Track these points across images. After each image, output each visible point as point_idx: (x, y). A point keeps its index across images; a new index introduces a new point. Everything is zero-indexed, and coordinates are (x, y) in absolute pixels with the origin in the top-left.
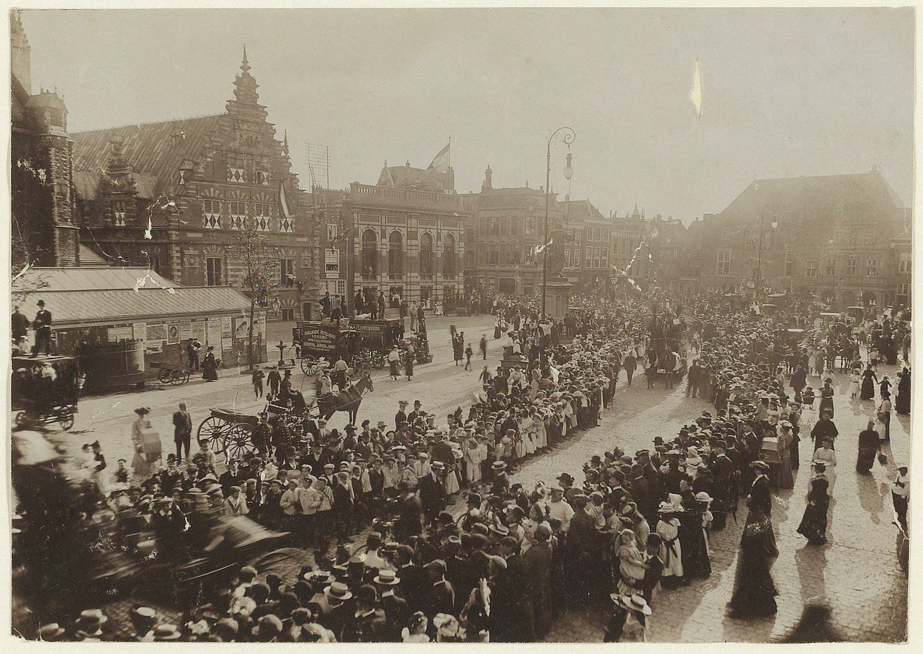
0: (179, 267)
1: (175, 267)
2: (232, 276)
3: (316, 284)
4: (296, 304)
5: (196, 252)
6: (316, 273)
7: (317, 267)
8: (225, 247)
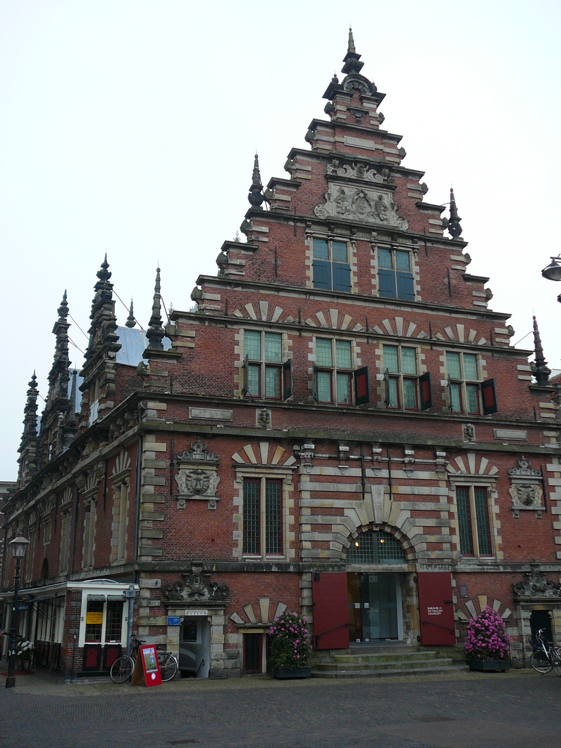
4: (507, 613)
8: (296, 447)
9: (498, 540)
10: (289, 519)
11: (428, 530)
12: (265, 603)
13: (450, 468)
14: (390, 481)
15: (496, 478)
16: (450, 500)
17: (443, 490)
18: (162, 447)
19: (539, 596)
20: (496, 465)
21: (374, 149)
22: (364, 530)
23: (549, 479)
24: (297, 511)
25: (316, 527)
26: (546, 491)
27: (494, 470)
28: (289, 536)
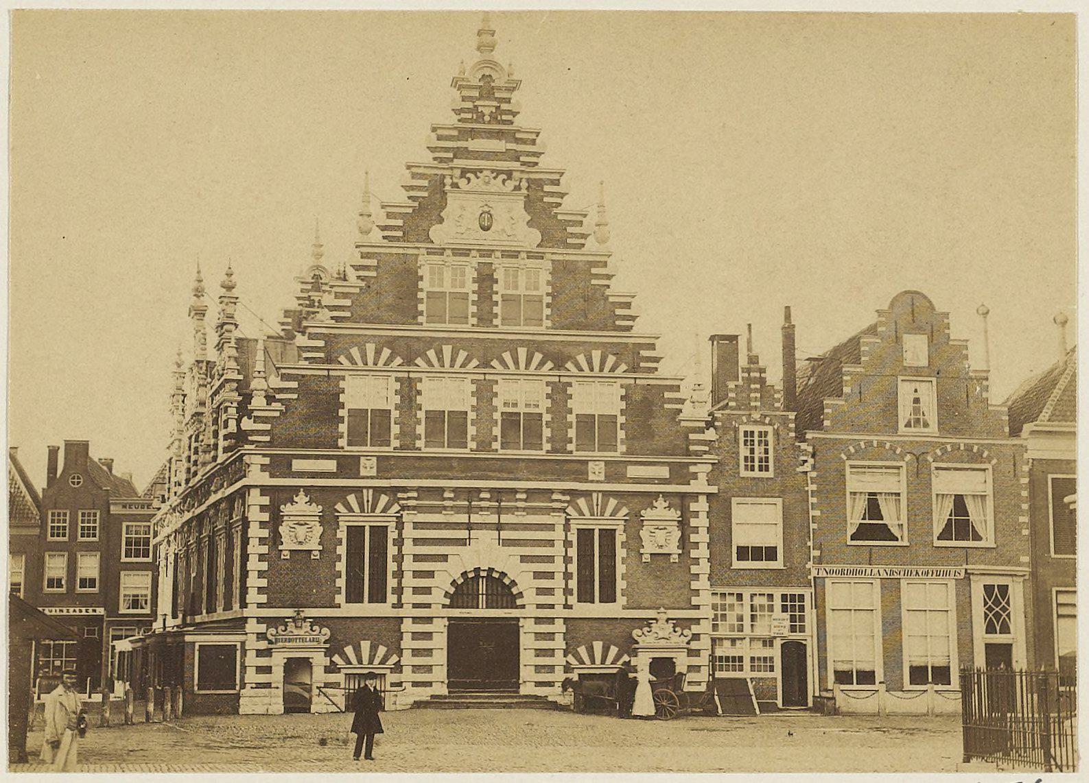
0: (264, 549)
1: (255, 548)
2: (417, 574)
3: (695, 601)
5: (316, 509)
6: (694, 569)
7: (702, 552)
8: (400, 495)
9: (621, 584)
10: (392, 566)
11: (538, 575)
12: (365, 646)
13: (570, 510)
14: (499, 527)
15: (626, 520)
16: (567, 544)
17: (558, 534)
18: (266, 501)
19: (663, 643)
20: (625, 505)
21: (504, 151)
22: (471, 575)
23: (692, 520)
24: (399, 558)
25: (417, 574)
26: (687, 533)
27: (625, 511)
28: (392, 583)
